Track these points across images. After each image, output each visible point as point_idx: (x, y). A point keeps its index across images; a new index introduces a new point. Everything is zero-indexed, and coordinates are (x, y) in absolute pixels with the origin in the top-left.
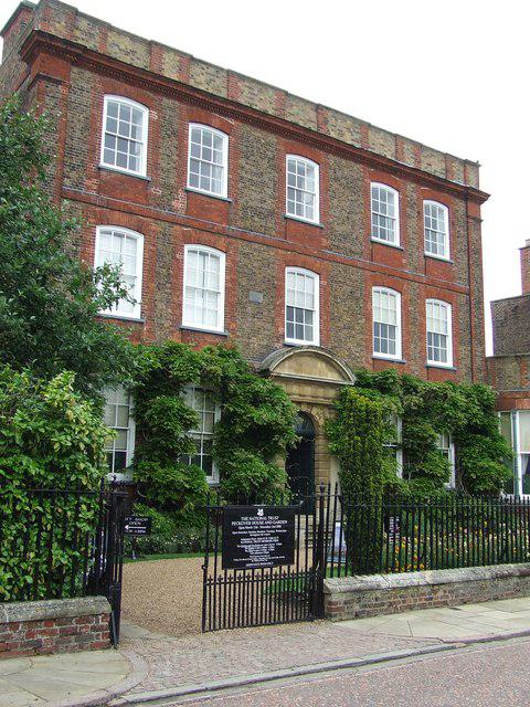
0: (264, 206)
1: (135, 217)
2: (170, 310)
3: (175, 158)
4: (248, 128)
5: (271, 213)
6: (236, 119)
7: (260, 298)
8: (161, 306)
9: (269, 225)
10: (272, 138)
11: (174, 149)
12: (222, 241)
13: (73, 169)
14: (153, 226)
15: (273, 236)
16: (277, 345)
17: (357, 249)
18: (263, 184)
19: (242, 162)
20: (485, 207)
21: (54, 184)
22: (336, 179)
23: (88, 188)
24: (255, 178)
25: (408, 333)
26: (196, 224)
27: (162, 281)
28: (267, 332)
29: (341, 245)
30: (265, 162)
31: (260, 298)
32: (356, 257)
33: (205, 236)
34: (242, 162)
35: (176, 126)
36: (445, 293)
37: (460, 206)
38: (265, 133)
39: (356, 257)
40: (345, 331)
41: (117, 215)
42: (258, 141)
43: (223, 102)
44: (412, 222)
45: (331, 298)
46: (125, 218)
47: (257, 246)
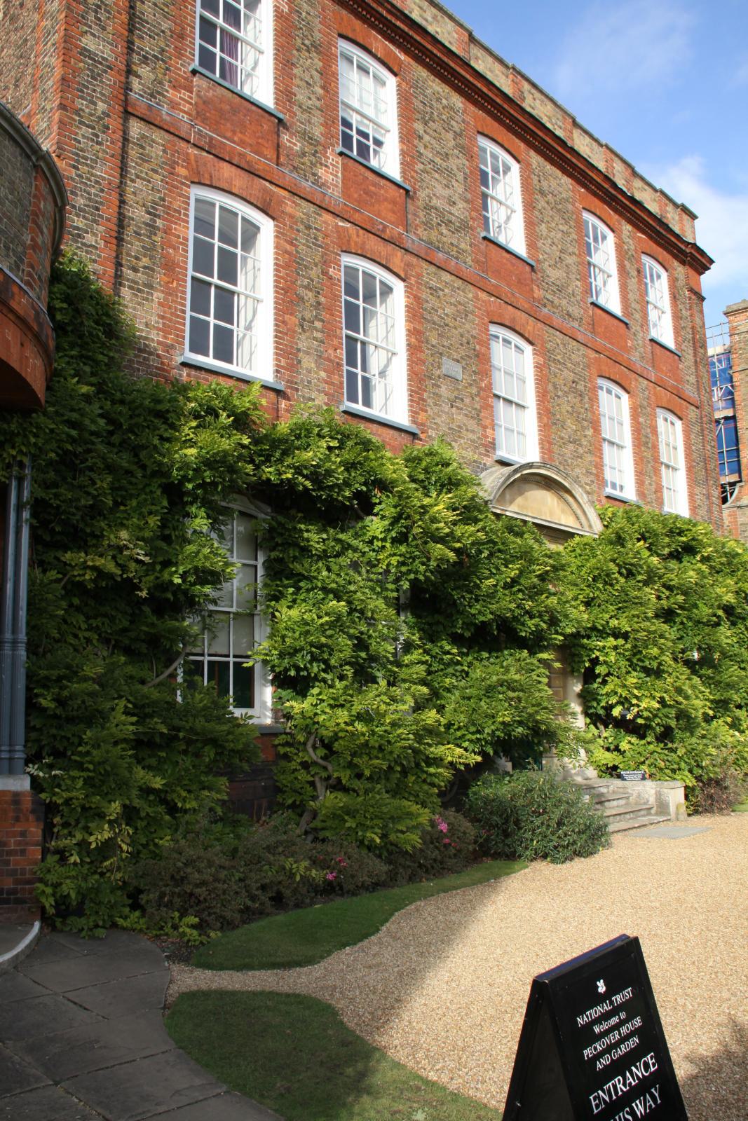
0: (454, 210)
1: (256, 179)
2: (323, 374)
3: (320, 91)
4: (422, 73)
5: (464, 227)
6: (406, 52)
7: (456, 370)
8: (308, 362)
9: (463, 246)
10: (457, 101)
11: (317, 76)
12: (398, 260)
13: (145, 60)
14: (289, 207)
15: (468, 265)
16: (489, 461)
17: (576, 311)
18: (449, 173)
19: (419, 127)
20: (706, 279)
21: (109, 79)
22: (542, 193)
23: (174, 105)
24: (437, 160)
25: (642, 459)
26: (357, 217)
27: (308, 315)
28: (471, 436)
29: (556, 301)
30: (450, 135)
31: (456, 370)
32: (576, 324)
33: (372, 244)
34: (419, 127)
35: (317, 36)
36: (677, 404)
37: (680, 270)
38: (447, 89)
39: (576, 324)
40: (571, 447)
41: (227, 171)
42: (439, 100)
43: (389, 11)
44: (633, 283)
45: (550, 387)
46: (239, 180)
47: (447, 277)
